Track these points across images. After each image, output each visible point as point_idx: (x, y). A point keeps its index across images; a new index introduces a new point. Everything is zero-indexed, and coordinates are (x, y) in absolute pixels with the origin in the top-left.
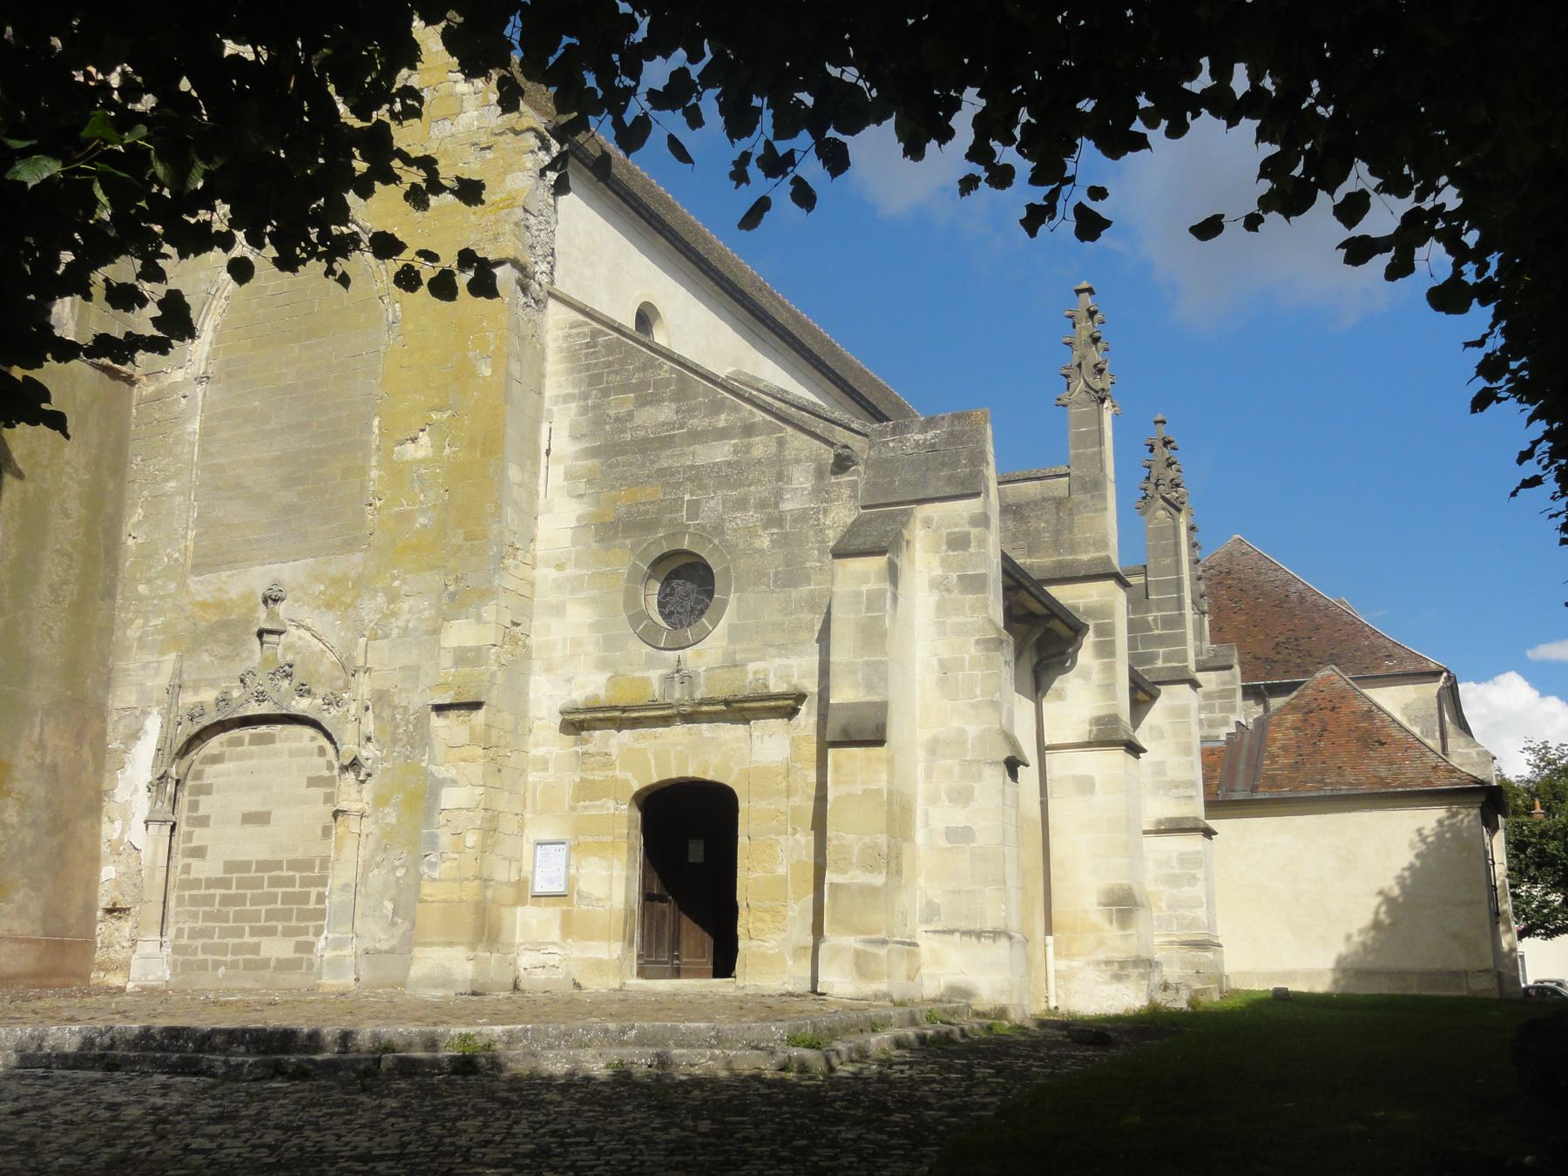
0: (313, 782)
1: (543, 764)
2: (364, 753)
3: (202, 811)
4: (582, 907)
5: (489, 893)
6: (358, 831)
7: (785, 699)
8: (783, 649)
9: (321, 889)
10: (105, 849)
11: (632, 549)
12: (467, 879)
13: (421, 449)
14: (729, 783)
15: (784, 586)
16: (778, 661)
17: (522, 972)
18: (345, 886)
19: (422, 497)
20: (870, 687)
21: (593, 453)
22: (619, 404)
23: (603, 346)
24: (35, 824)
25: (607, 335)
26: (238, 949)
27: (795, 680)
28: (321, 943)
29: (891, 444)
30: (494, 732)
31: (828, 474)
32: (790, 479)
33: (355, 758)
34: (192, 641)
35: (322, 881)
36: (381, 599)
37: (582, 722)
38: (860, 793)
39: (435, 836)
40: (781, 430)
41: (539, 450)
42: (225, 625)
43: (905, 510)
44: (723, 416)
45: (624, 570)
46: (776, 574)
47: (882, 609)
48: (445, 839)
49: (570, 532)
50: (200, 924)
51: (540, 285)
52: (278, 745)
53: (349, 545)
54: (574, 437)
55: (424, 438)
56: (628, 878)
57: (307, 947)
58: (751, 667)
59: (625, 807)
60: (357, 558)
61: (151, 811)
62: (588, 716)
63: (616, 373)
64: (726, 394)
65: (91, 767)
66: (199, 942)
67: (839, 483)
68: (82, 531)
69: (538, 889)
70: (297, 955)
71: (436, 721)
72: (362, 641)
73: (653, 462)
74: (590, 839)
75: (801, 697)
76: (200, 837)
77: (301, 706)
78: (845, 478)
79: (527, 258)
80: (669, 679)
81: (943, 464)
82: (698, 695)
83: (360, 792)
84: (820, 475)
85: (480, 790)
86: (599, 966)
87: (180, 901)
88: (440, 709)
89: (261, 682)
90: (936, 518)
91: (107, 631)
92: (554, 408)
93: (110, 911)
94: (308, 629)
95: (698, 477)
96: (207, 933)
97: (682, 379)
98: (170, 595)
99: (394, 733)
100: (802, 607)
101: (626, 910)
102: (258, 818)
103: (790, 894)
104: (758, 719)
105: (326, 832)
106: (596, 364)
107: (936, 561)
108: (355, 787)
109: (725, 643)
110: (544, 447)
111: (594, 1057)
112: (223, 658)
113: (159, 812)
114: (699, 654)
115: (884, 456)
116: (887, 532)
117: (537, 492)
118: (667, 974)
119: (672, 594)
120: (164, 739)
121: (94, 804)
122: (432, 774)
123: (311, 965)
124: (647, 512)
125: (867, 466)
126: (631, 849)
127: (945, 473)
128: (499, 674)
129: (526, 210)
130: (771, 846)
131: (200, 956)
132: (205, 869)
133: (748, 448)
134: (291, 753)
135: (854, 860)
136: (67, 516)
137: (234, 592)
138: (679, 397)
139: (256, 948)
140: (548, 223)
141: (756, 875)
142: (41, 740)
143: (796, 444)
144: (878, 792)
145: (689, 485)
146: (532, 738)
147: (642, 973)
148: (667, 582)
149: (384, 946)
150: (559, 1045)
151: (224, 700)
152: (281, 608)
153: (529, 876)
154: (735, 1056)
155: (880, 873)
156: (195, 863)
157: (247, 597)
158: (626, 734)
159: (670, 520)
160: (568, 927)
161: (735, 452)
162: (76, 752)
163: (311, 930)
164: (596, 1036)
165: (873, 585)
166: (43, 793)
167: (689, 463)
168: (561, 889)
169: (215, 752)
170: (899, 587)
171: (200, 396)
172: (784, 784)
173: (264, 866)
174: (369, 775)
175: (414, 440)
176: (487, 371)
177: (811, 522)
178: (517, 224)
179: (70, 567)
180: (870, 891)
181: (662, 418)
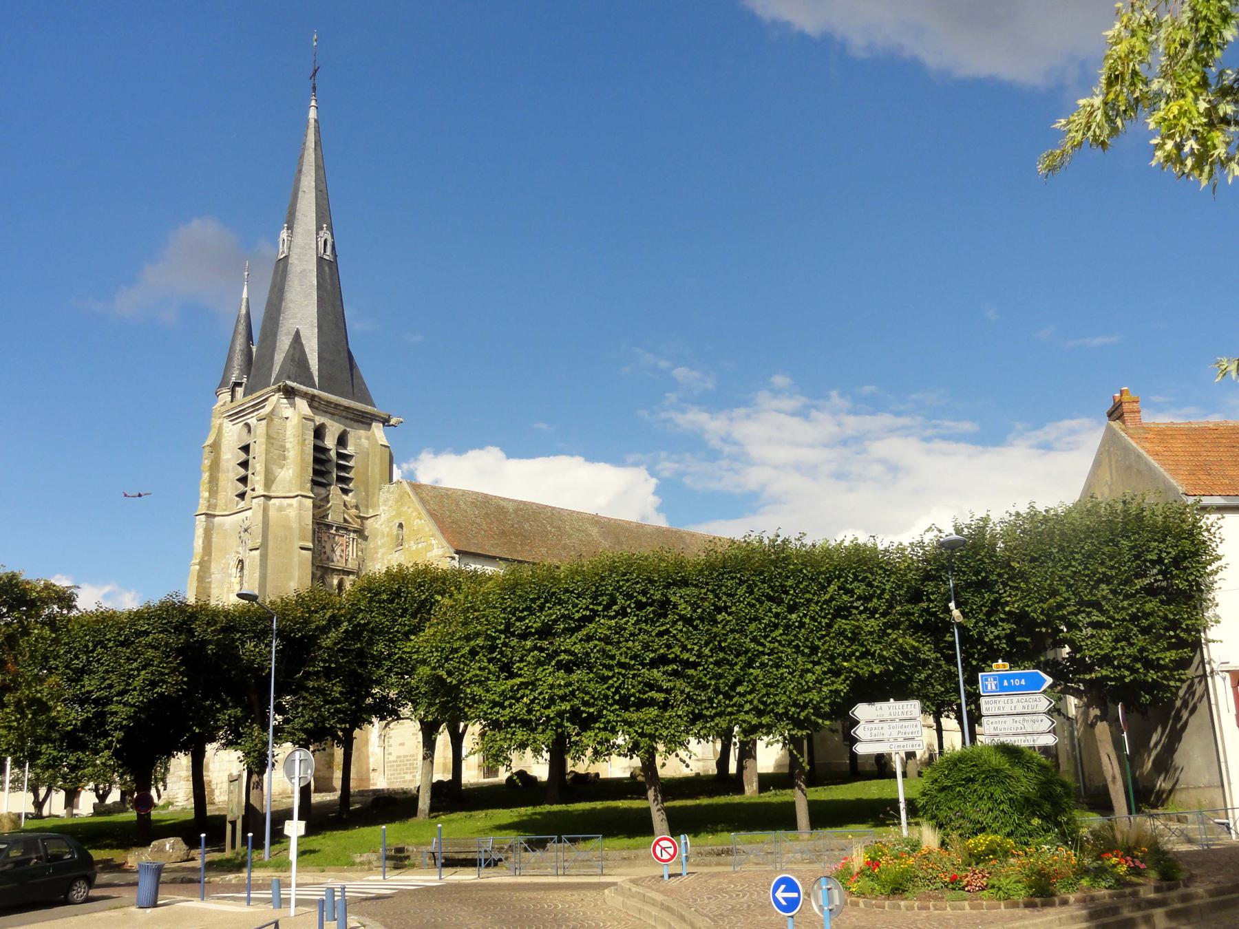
0: (414, 734)
35: (416, 760)
76: (391, 750)
102: (402, 744)
132: (392, 758)
139: (404, 777)
173: (405, 756)
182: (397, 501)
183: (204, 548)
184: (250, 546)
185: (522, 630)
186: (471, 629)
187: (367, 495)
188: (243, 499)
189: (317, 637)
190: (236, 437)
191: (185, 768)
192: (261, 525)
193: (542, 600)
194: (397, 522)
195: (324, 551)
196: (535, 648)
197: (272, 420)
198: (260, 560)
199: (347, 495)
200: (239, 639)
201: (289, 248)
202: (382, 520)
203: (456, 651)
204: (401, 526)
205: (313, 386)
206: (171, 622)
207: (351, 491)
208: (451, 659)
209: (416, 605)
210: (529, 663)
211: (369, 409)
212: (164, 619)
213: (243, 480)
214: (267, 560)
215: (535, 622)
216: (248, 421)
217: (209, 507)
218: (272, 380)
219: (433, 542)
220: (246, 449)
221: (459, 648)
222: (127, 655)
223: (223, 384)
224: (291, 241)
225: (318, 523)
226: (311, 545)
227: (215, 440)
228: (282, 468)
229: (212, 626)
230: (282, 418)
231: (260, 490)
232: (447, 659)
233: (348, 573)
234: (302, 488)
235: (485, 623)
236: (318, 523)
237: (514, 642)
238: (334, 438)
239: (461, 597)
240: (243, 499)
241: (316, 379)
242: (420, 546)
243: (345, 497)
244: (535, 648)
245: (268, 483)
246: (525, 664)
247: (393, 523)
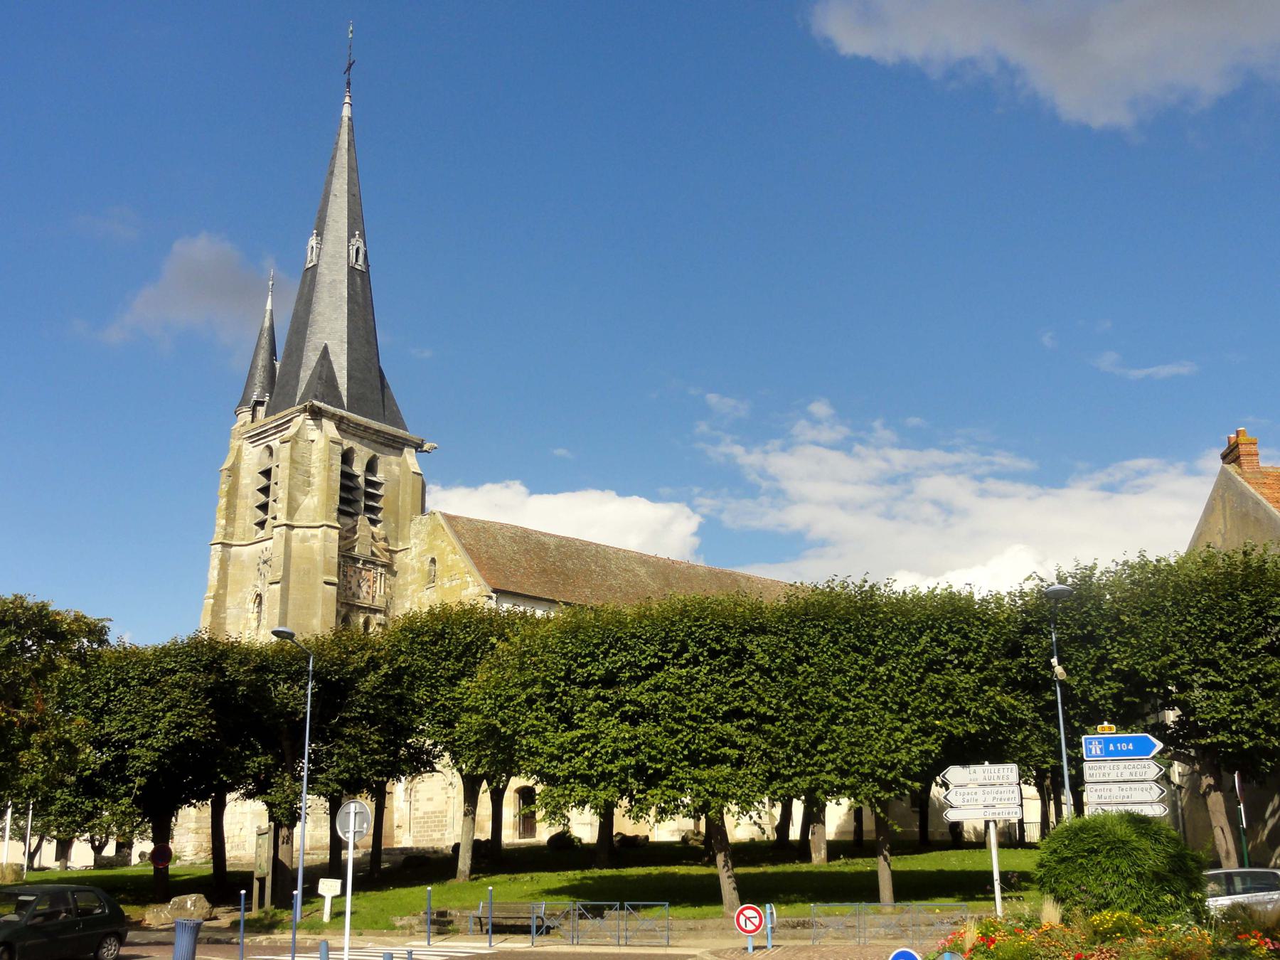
0: (443, 789)
26: (428, 836)
28: (446, 833)
35: (446, 816)
57: (443, 835)
93: (398, 827)
96: (420, 832)
102: (430, 799)
105: (446, 803)
132: (419, 814)
139: (432, 835)
173: (433, 813)
182: (429, 534)
183: (219, 581)
184: (270, 578)
185: (583, 677)
186: (528, 676)
187: (397, 526)
188: (263, 528)
189: (354, 681)
190: (256, 461)
191: (194, 820)
192: (282, 556)
193: (606, 646)
195: (349, 586)
196: (597, 697)
197: (297, 443)
200: (271, 680)
201: (319, 256)
202: (413, 554)
203: (510, 699)
204: (433, 561)
205: (342, 407)
206: (201, 661)
207: (380, 522)
208: (506, 708)
209: (461, 648)
210: (591, 713)
211: (400, 432)
212: (193, 656)
213: (264, 507)
215: (598, 669)
216: (270, 443)
217: (225, 536)
218: (297, 400)
219: (469, 579)
220: (267, 473)
221: (515, 695)
222: (153, 694)
223: (244, 402)
224: (320, 249)
225: (343, 556)
226: (336, 580)
227: (234, 463)
228: (306, 495)
229: (245, 666)
230: (307, 440)
231: (282, 519)
232: (501, 707)
233: (375, 611)
234: (328, 518)
235: (543, 669)
236: (343, 556)
237: (575, 690)
239: (517, 639)
240: (263, 528)
241: (345, 400)
242: (454, 583)
243: (373, 528)
244: (597, 697)
245: (291, 512)
246: (586, 714)
247: (425, 558)
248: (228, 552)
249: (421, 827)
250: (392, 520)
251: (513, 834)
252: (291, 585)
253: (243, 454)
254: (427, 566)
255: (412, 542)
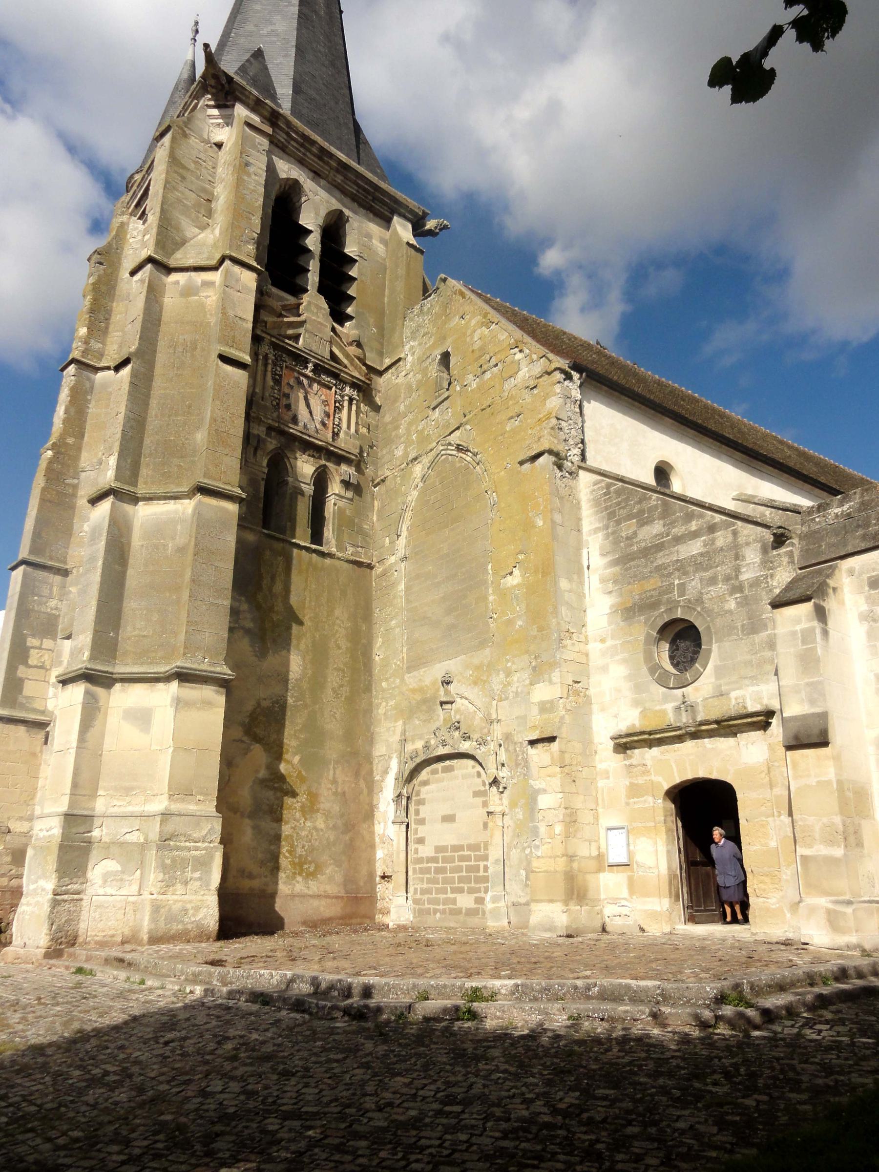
0: (476, 794)
1: (606, 775)
2: (501, 774)
3: (422, 815)
4: (640, 873)
5: (575, 865)
6: (501, 824)
7: (757, 716)
8: (755, 679)
9: (485, 863)
10: (377, 840)
11: (645, 623)
12: (558, 856)
13: (515, 579)
14: (728, 779)
15: (749, 634)
16: (751, 689)
17: (607, 920)
18: (497, 861)
19: (518, 609)
20: (812, 702)
21: (615, 563)
22: (628, 528)
23: (614, 493)
24: (335, 827)
25: (615, 485)
26: (446, 901)
27: (765, 701)
28: (488, 898)
29: (817, 520)
30: (567, 756)
31: (770, 549)
32: (744, 557)
33: (495, 778)
34: (409, 713)
35: (485, 858)
36: (502, 675)
37: (625, 744)
38: (814, 784)
39: (536, 828)
40: (734, 524)
41: (583, 567)
42: (425, 701)
43: (831, 566)
44: (694, 523)
45: (642, 638)
46: (743, 626)
47: (814, 641)
48: (543, 829)
49: (606, 617)
50: (425, 886)
51: (572, 463)
52: (456, 772)
53: (482, 645)
54: (603, 555)
55: (516, 572)
56: (668, 852)
57: (480, 901)
58: (733, 695)
59: (660, 801)
60: (487, 651)
61: (395, 817)
62: (628, 739)
63: (623, 508)
64: (695, 508)
65: (365, 791)
66: (425, 897)
67: (779, 554)
68: (348, 656)
69: (612, 860)
70: (476, 906)
71: (532, 751)
72: (494, 703)
73: (652, 562)
74: (640, 825)
75: (770, 714)
77: (465, 747)
78: (783, 550)
79: (560, 448)
80: (678, 708)
81: (858, 526)
82: (700, 718)
83: (501, 799)
84: (764, 551)
85: (561, 795)
86: (654, 915)
87: (414, 870)
88: (532, 743)
89: (444, 734)
90: (857, 568)
91: (369, 711)
92: (590, 539)
93: (383, 877)
94: (466, 699)
95: (682, 567)
97: (665, 504)
98: (397, 687)
99: (516, 760)
100: (764, 648)
101: (670, 875)
102: (449, 819)
103: (782, 863)
104: (742, 732)
105: (485, 825)
106: (611, 506)
107: (861, 600)
108: (498, 796)
109: (713, 680)
110: (585, 565)
111: (559, 1010)
112: (425, 721)
113: (399, 817)
114: (697, 690)
115: (813, 529)
116: (813, 583)
117: (584, 594)
118: (716, 918)
119: (677, 650)
120: (400, 772)
121: (369, 815)
122: (532, 787)
123: (484, 913)
124: (652, 596)
125: (801, 538)
126: (668, 831)
127: (860, 532)
128: (567, 716)
129: (558, 419)
130: (763, 826)
131: (427, 906)
132: (426, 851)
133: (713, 541)
134: (464, 777)
135: (817, 836)
136: (339, 648)
137: (427, 682)
138: (663, 517)
139: (454, 901)
140: (576, 424)
141: (755, 848)
142: (334, 778)
143: (746, 532)
144: (829, 782)
145: (677, 574)
146: (597, 757)
147: (692, 919)
148: (673, 643)
149: (523, 900)
150: (542, 998)
151: (427, 747)
152: (451, 687)
153: (605, 851)
154: (670, 1014)
155: (839, 846)
156: (420, 847)
157: (434, 683)
158: (655, 751)
159: (667, 599)
160: (633, 887)
161: (705, 546)
162: (356, 784)
163: (482, 890)
164: (568, 991)
165: (805, 625)
166: (338, 810)
167: (675, 559)
168: (623, 860)
169: (425, 779)
170: (831, 623)
171: (403, 569)
172: (767, 779)
173: (456, 848)
174: (505, 788)
175: (511, 574)
176: (540, 523)
177: (763, 585)
178: (552, 428)
179: (344, 677)
180: (832, 861)
181: (655, 532)
187: (381, 329)
194: (437, 354)
198: (131, 383)
199: (342, 325)
202: (408, 367)
207: (350, 318)
214: (149, 388)
217: (85, 353)
226: (247, 359)
227: (109, 245)
230: (207, 142)
233: (340, 459)
238: (317, 214)
242: (488, 375)
248: (89, 379)
249: (429, 881)
250: (371, 321)
251: (670, 912)
252: (158, 370)
253: (129, 236)
254: (434, 369)
255: (407, 348)
